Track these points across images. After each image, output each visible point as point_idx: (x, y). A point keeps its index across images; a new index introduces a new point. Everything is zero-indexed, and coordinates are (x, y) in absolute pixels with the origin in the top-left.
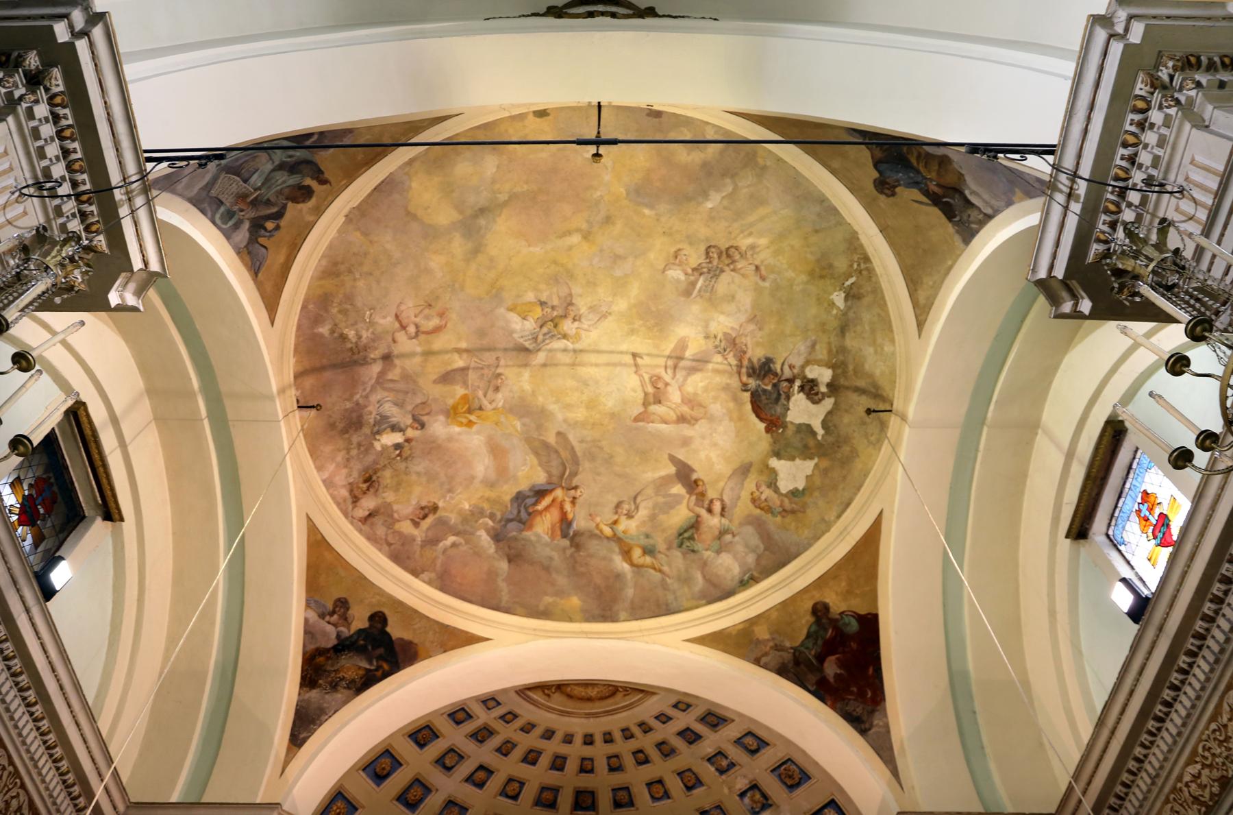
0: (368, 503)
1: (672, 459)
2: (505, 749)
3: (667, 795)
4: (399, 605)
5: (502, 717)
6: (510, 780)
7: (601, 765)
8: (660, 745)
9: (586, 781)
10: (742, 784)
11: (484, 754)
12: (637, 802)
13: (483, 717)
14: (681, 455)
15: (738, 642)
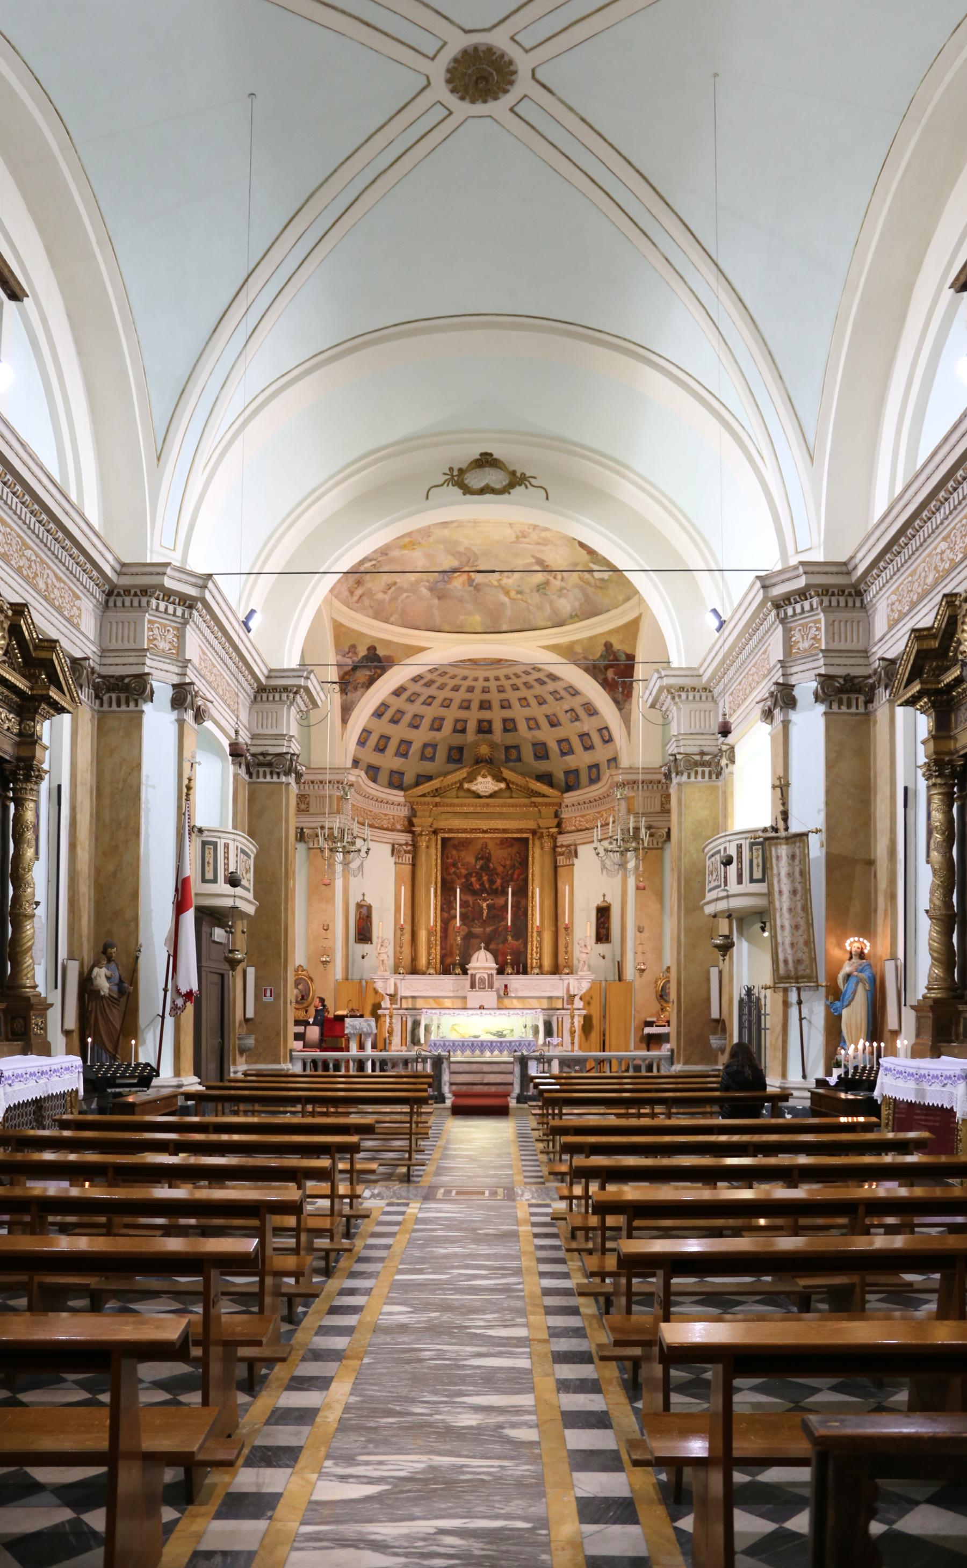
0: (359, 592)
1: (533, 557)
2: (441, 688)
3: (528, 705)
4: (381, 641)
5: (440, 675)
6: (445, 699)
7: (494, 689)
8: (525, 684)
9: (485, 697)
10: (567, 707)
11: (432, 691)
12: (513, 706)
13: (429, 677)
14: (539, 555)
15: (567, 651)
